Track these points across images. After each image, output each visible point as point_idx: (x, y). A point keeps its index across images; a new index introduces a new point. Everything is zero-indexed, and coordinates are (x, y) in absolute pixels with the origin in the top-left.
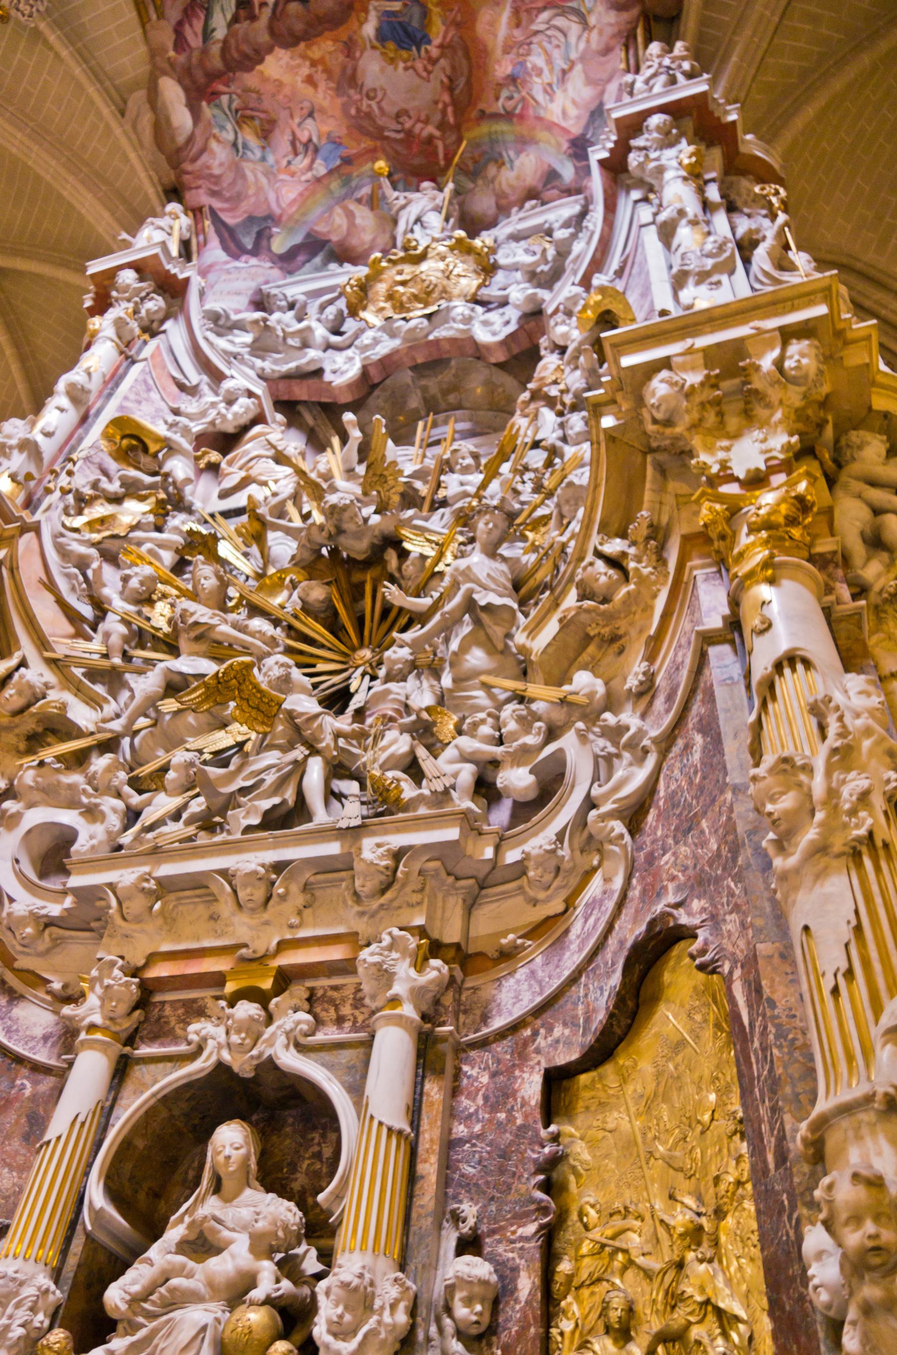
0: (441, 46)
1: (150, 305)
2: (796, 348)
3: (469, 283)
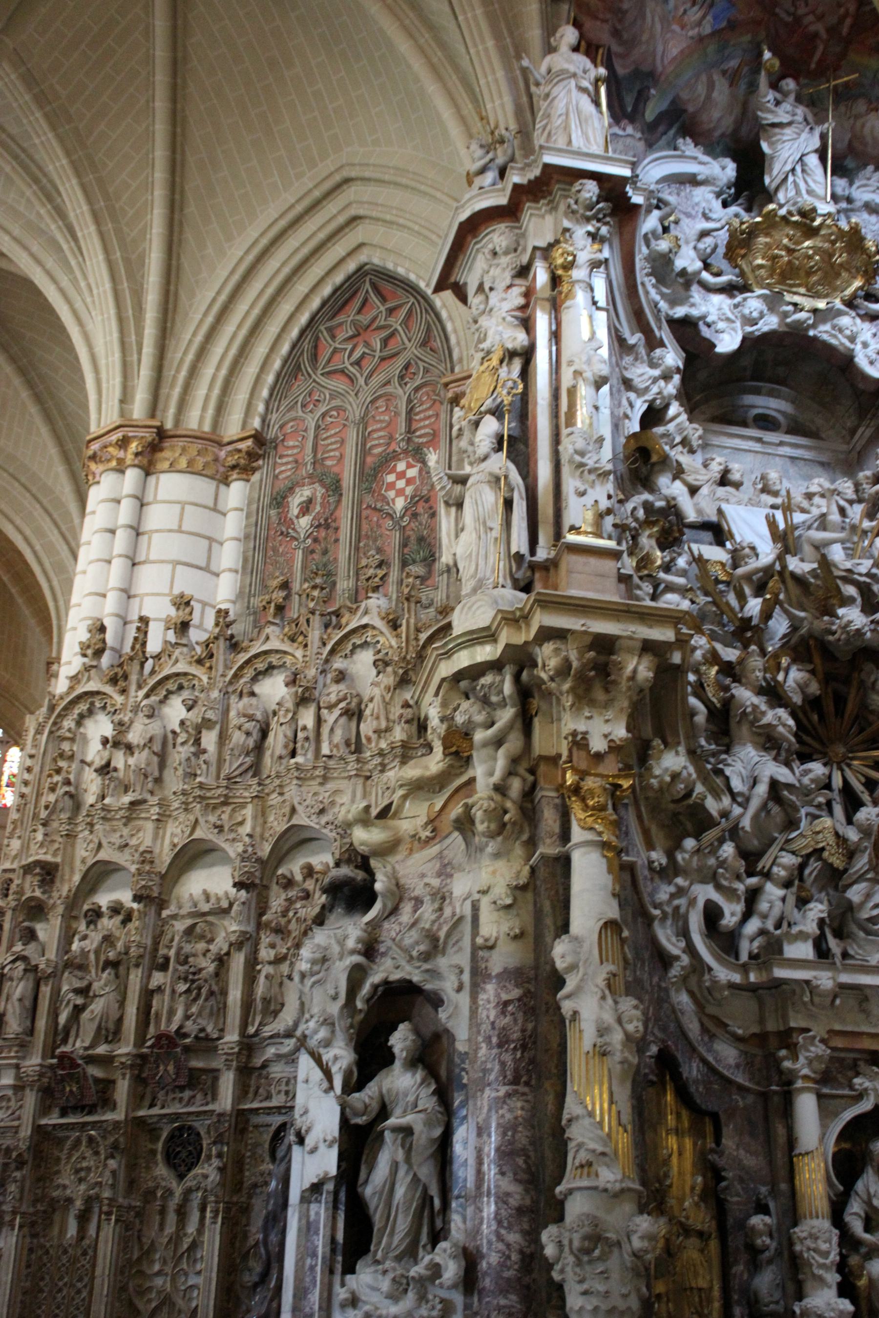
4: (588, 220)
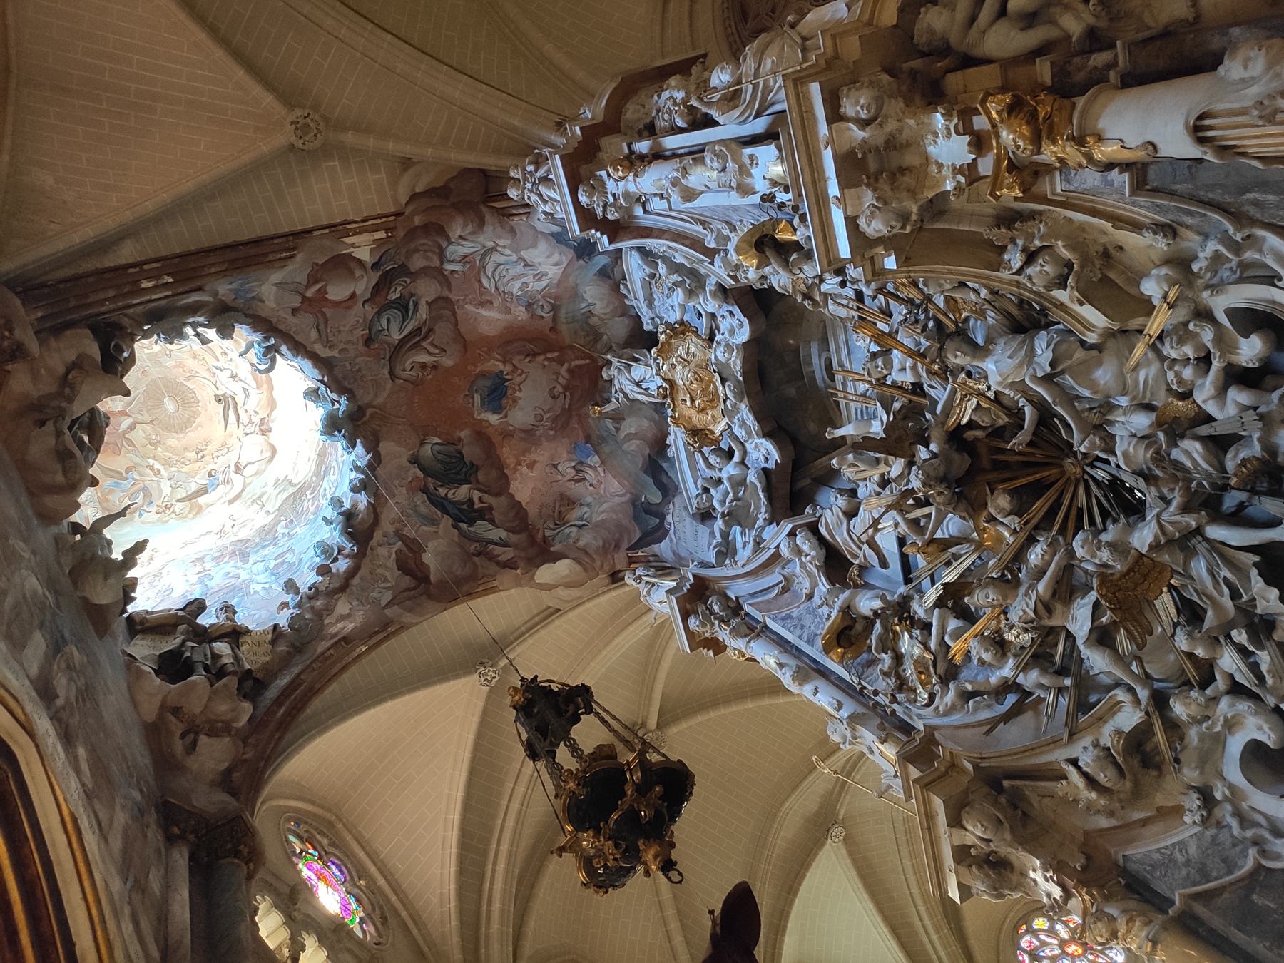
0: (504, 362)
1: (716, 608)
2: (848, 108)
3: (693, 346)
4: (713, 624)
